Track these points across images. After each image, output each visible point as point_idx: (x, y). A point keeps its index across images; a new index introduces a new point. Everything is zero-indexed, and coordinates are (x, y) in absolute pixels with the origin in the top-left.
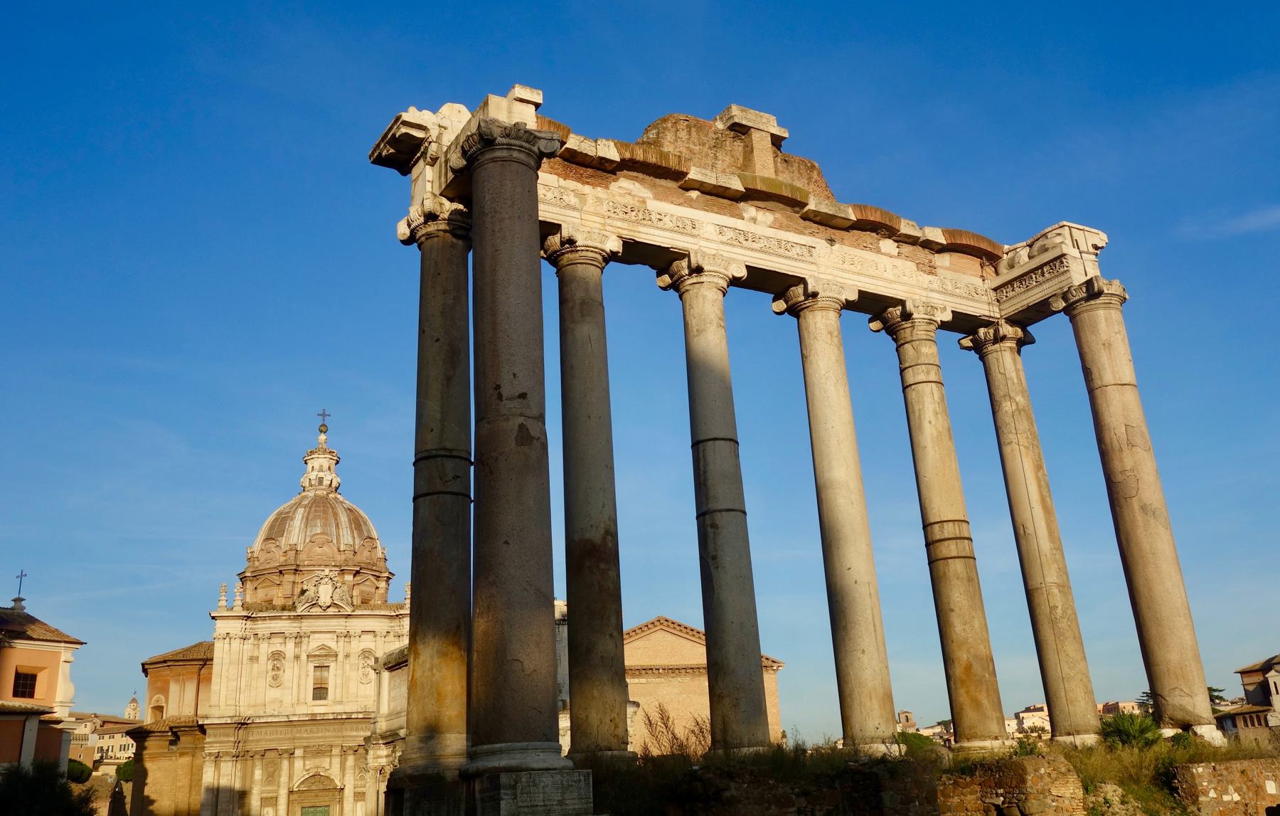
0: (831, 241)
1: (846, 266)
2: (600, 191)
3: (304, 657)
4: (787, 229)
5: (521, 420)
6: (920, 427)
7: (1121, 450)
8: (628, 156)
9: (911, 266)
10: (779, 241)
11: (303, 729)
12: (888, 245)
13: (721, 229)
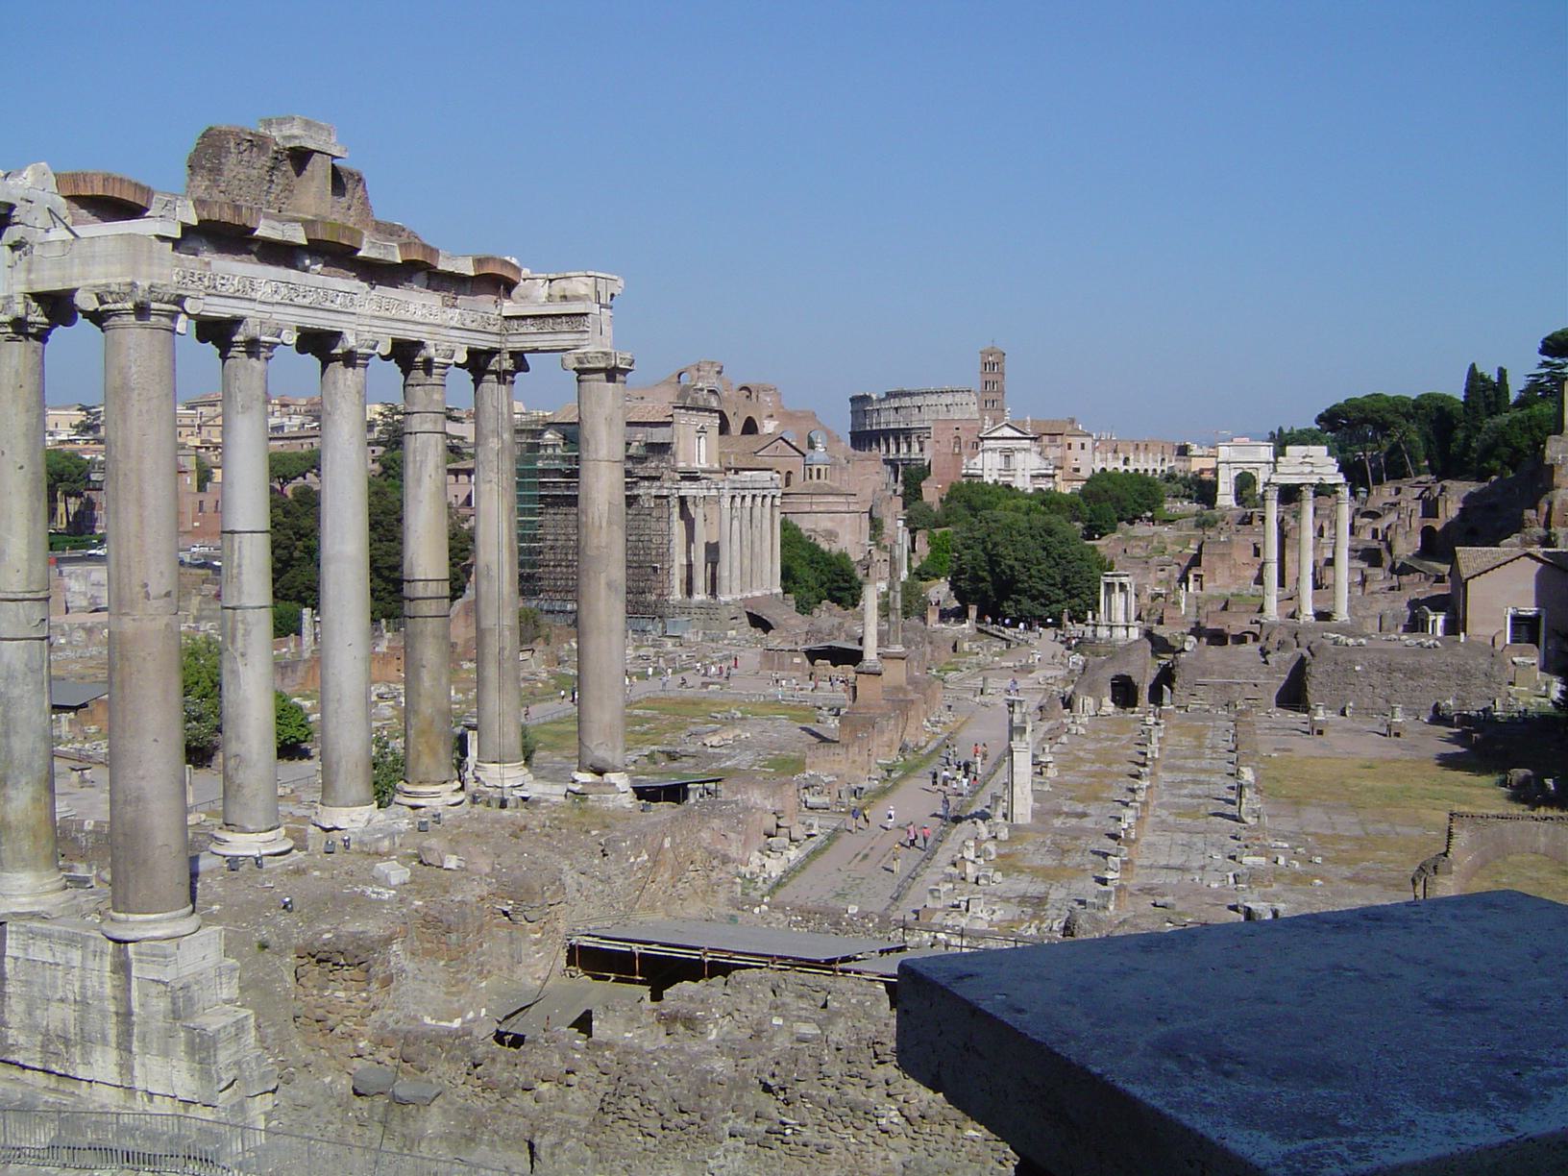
1: (382, 313)
6: (419, 481)
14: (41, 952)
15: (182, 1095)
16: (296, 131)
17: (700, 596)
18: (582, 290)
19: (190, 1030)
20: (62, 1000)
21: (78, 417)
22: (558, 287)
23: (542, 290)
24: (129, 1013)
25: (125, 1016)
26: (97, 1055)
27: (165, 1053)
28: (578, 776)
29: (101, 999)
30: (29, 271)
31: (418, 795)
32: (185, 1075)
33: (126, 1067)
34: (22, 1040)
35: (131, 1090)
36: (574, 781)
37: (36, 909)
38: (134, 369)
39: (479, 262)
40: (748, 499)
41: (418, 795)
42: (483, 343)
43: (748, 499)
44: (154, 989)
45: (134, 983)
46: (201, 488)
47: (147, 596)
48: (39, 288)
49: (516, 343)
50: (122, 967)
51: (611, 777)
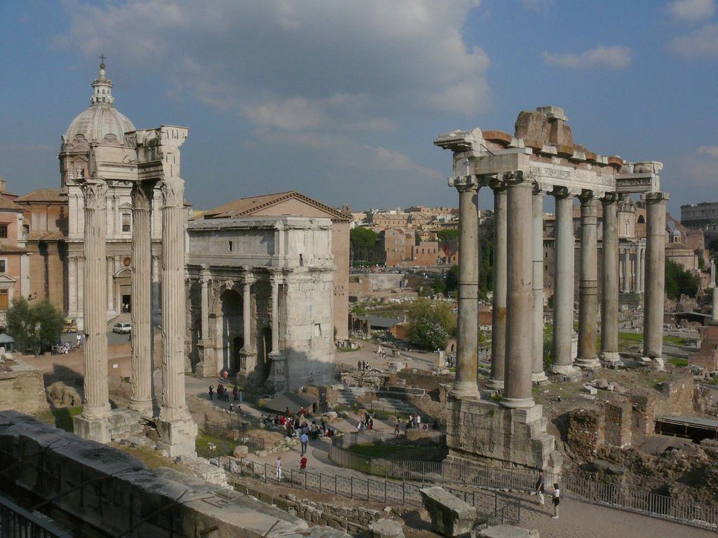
0: (575, 168)
3: (117, 209)
5: (529, 293)
6: (587, 243)
7: (655, 261)
8: (527, 145)
10: (561, 171)
11: (118, 246)
12: (589, 166)
14: (475, 411)
15: (529, 465)
16: (552, 112)
18: (649, 169)
19: (533, 441)
20: (482, 428)
21: (365, 216)
22: (638, 168)
23: (631, 169)
24: (510, 434)
25: (508, 435)
26: (495, 448)
27: (524, 450)
28: (643, 359)
29: (499, 428)
30: (475, 167)
31: (584, 363)
32: (531, 458)
33: (507, 454)
34: (465, 442)
36: (643, 361)
37: (473, 395)
38: (519, 202)
39: (610, 159)
41: (584, 363)
42: (611, 189)
44: (521, 426)
45: (512, 423)
46: (417, 244)
47: (523, 283)
48: (479, 173)
49: (621, 189)
50: (508, 418)
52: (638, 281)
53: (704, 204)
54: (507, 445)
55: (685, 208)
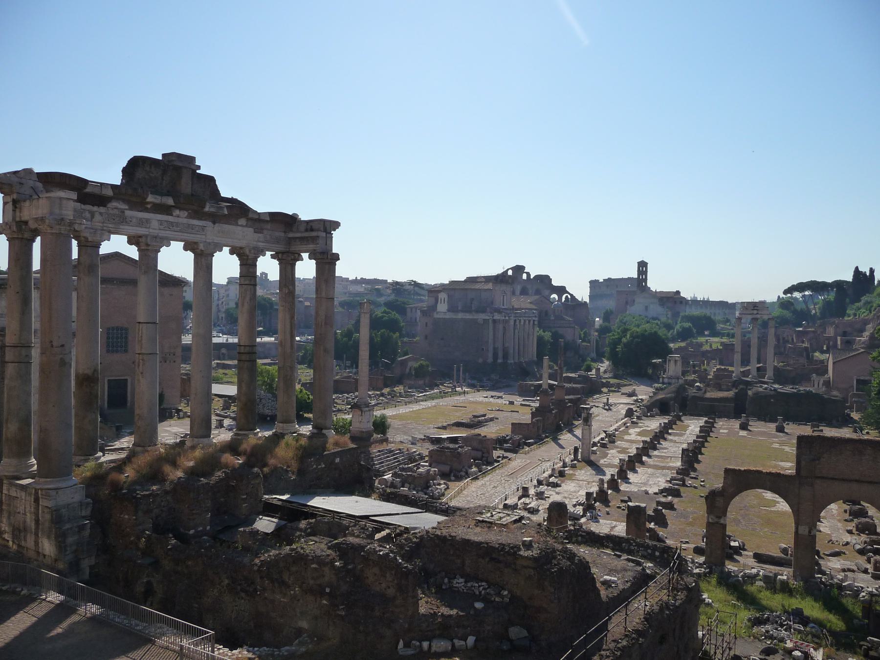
0: (214, 223)
2: (102, 209)
4: (194, 218)
9: (251, 230)
12: (242, 221)
13: (161, 222)
17: (500, 361)
26: (29, 535)
35: (38, 553)
40: (522, 322)
43: (522, 322)
47: (52, 346)
49: (293, 249)
51: (324, 431)
52: (512, 351)
53: (609, 279)
54: (36, 534)
55: (594, 284)
